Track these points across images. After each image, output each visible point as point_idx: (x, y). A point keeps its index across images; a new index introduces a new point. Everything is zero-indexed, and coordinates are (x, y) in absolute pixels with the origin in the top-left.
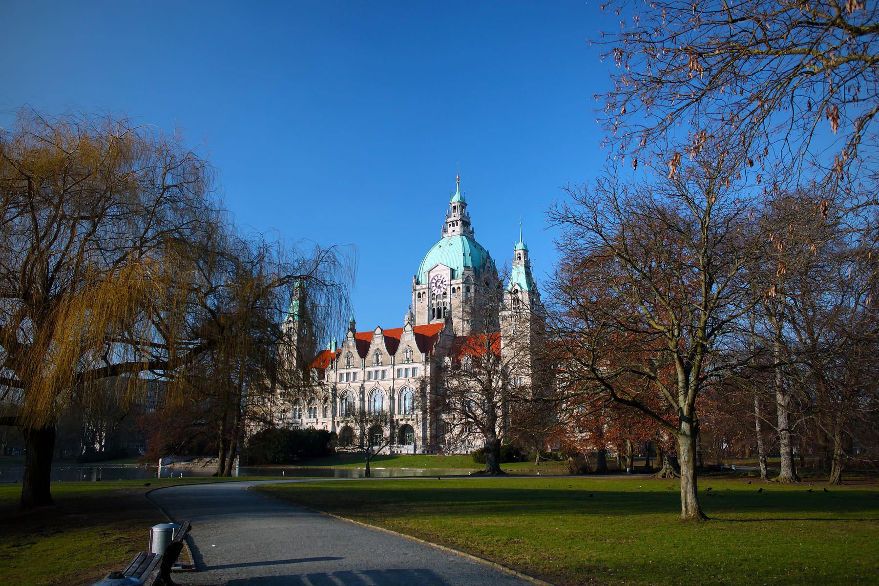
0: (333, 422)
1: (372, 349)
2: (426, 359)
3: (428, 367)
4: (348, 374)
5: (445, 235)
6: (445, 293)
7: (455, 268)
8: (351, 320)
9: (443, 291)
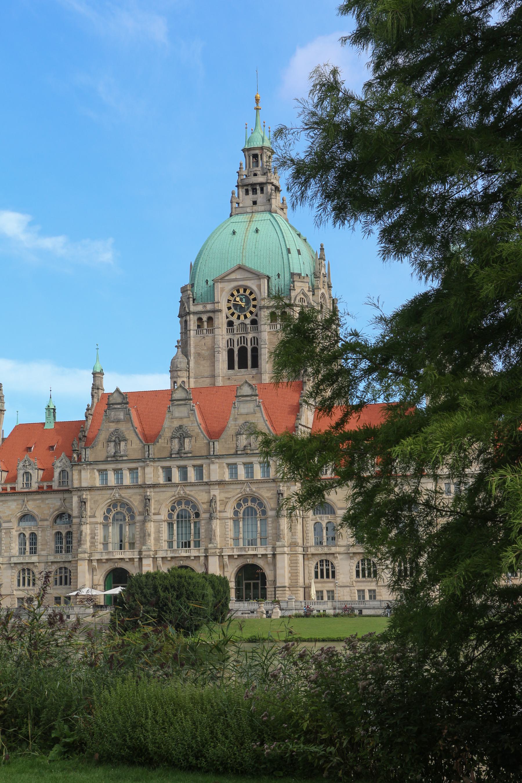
1: (169, 426)
6: (254, 322)
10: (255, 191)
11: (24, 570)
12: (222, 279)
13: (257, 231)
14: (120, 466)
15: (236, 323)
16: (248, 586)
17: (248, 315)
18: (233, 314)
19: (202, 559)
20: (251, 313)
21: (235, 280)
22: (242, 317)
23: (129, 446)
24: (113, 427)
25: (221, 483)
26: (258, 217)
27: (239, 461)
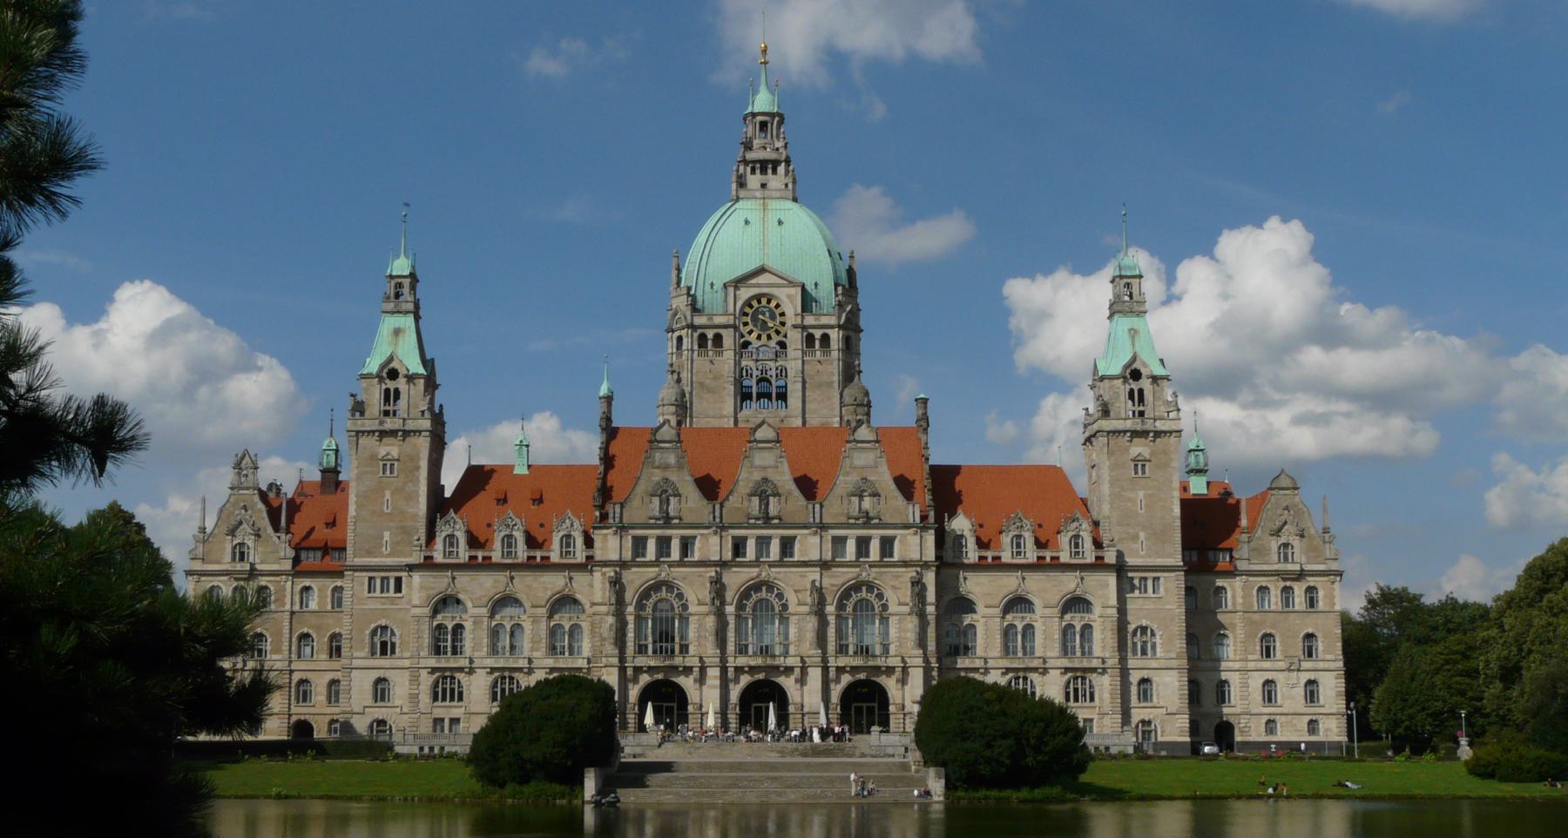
0: (622, 670)
1: (747, 478)
2: (924, 518)
3: (930, 538)
4: (663, 543)
5: (742, 193)
6: (782, 345)
7: (810, 287)
8: (604, 390)
9: (776, 338)
10: (764, 171)
11: (503, 678)
12: (739, 282)
13: (780, 223)
14: (668, 532)
15: (756, 344)
16: (859, 711)
17: (773, 335)
18: (750, 332)
19: (797, 671)
20: (778, 332)
21: (758, 286)
22: (764, 337)
23: (683, 505)
24: (657, 476)
25: (824, 565)
26: (773, 204)
27: (852, 534)
